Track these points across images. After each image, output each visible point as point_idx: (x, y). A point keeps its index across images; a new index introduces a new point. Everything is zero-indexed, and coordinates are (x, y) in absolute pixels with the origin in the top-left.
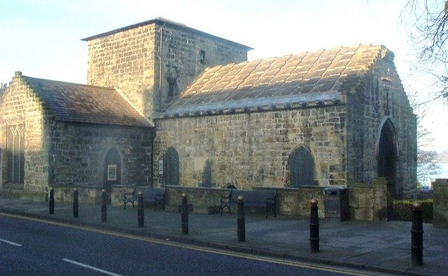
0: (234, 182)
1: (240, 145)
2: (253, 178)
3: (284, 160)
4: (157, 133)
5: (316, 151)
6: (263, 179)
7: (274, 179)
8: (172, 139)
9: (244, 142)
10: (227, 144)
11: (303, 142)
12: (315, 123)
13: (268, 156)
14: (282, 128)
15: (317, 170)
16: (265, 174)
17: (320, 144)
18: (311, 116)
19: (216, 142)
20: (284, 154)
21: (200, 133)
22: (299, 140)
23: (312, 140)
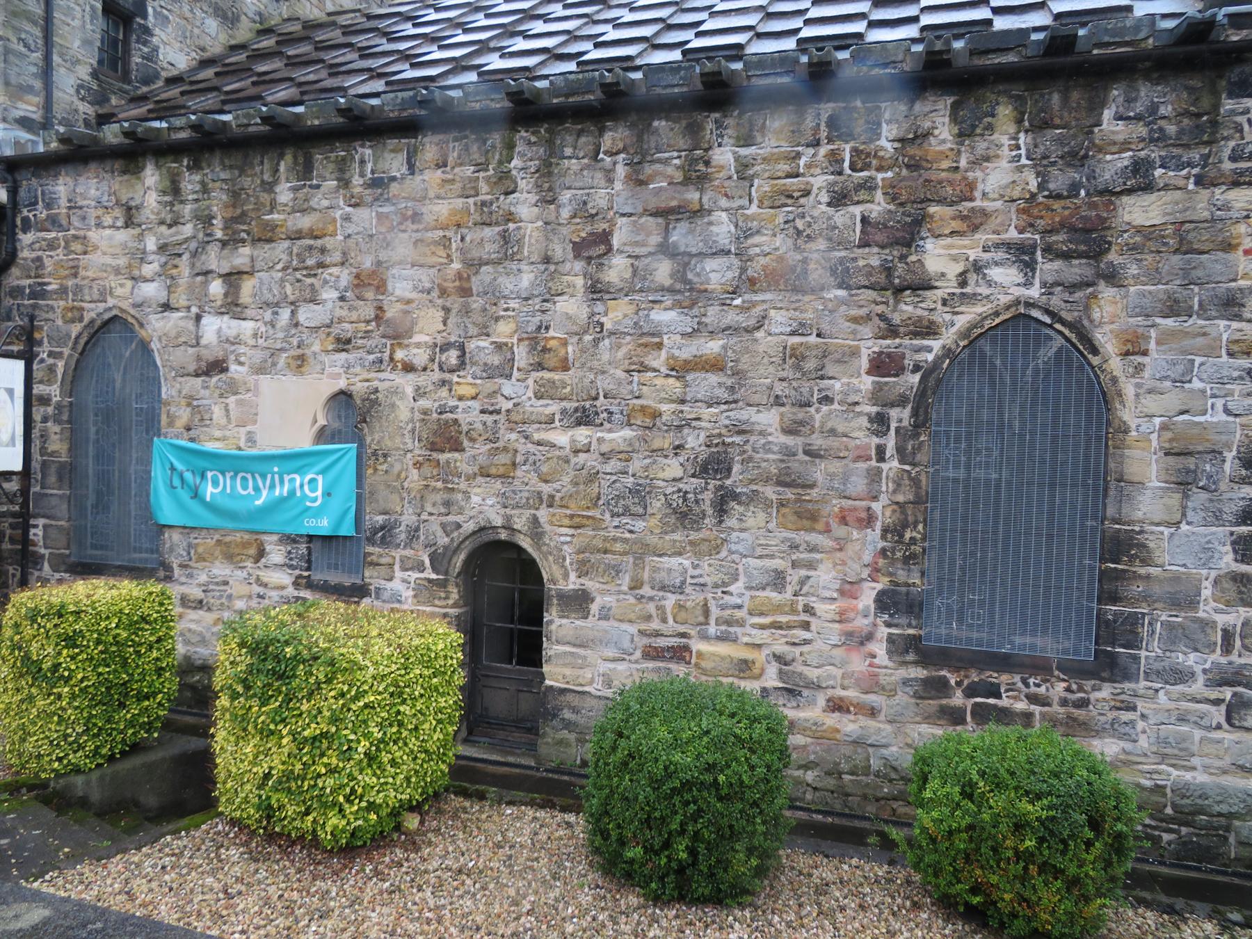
0: (520, 523)
1: (572, 306)
2: (657, 504)
3: (877, 396)
4: (26, 238)
5: (1134, 348)
6: (721, 509)
7: (808, 517)
8: (117, 271)
9: (597, 291)
10: (476, 303)
11: (1035, 292)
12: (1140, 168)
13: (764, 376)
14: (878, 206)
15: (1133, 469)
16: (736, 478)
17: (1174, 308)
18: (1110, 125)
19: (401, 286)
20: (883, 365)
21: (297, 236)
22: (1006, 276)
23: (1112, 277)
